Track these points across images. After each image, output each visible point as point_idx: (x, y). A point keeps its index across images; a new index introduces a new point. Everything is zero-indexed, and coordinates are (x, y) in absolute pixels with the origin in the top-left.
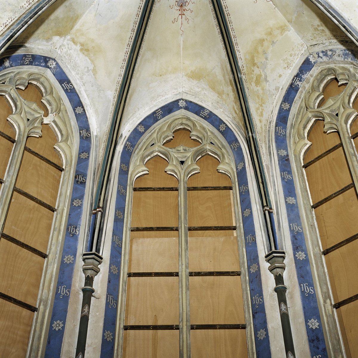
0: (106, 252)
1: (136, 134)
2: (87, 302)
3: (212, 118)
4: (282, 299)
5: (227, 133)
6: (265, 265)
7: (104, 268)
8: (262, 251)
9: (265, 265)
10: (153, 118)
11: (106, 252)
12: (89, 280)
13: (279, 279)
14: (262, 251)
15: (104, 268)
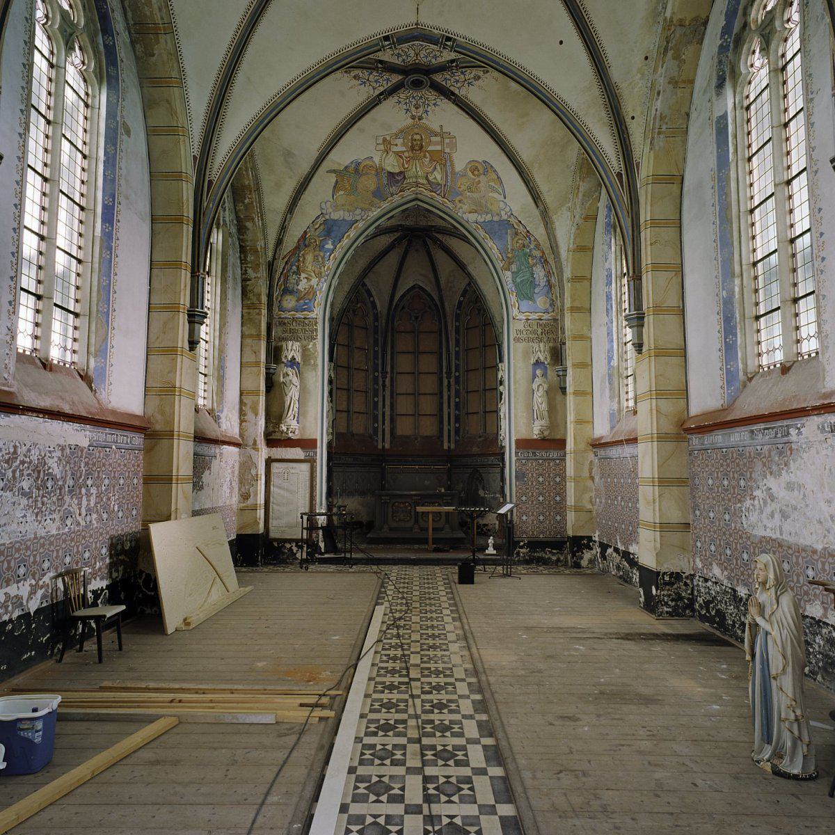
0: (389, 370)
1: (397, 306)
2: (384, 390)
3: (429, 295)
4: (449, 390)
5: (436, 305)
6: (445, 375)
7: (388, 375)
8: (444, 371)
9: (445, 375)
10: (403, 296)
11: (389, 370)
12: (384, 382)
13: (449, 382)
14: (444, 371)
15: (388, 375)
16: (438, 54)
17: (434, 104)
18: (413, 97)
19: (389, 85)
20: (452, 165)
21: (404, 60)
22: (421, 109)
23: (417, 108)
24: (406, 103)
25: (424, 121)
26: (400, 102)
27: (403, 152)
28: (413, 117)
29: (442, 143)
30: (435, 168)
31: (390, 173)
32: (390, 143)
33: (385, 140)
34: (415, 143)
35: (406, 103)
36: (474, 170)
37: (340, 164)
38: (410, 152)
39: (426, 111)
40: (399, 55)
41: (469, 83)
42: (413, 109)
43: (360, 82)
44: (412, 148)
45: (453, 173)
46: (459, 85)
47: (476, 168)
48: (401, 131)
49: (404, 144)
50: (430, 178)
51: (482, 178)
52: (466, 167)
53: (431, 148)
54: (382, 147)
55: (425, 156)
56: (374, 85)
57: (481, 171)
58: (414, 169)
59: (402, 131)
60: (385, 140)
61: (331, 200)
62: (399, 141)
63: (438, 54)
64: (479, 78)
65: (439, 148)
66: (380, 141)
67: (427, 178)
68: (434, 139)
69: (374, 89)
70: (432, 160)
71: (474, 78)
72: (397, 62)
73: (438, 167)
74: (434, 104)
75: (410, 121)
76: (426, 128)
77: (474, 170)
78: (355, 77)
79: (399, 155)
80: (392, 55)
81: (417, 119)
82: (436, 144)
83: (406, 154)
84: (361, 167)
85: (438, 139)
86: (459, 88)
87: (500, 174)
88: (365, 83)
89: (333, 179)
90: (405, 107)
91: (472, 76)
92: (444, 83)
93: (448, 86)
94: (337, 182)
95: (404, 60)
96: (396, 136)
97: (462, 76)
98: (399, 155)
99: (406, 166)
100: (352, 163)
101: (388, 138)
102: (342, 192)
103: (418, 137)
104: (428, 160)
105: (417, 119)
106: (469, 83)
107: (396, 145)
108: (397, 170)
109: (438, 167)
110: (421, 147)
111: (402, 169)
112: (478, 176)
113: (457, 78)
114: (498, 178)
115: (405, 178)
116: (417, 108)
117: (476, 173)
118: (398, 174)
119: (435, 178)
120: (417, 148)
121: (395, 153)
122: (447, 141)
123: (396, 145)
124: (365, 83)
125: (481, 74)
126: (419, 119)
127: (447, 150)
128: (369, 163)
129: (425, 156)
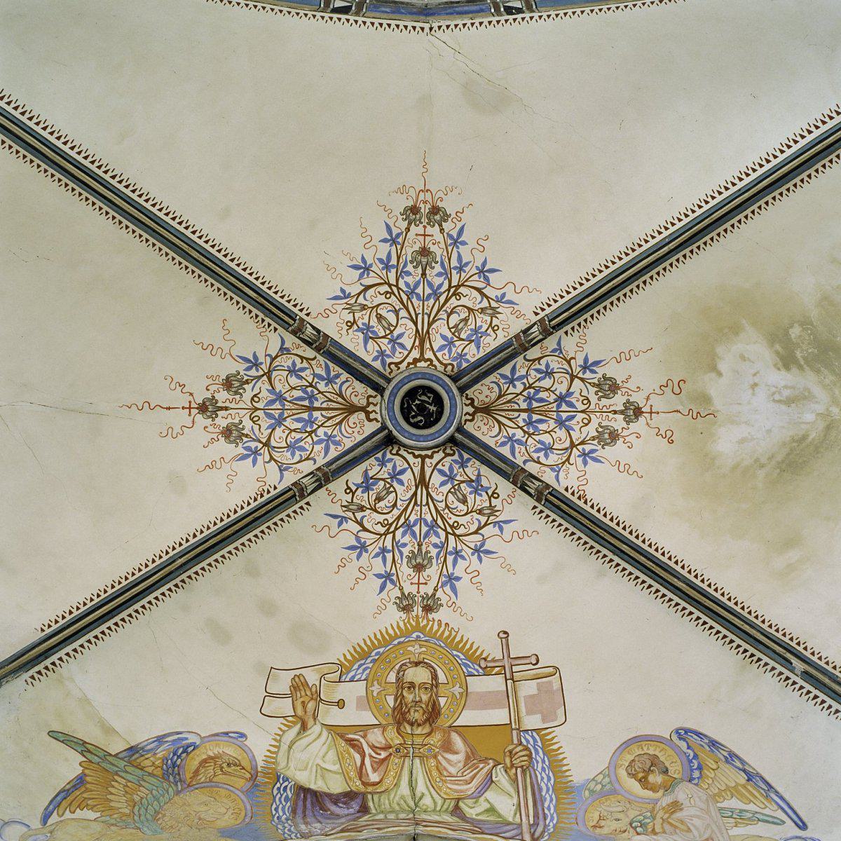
16: (482, 321)
17: (477, 550)
18: (409, 527)
19: (333, 453)
20: (556, 765)
21: (382, 354)
22: (433, 572)
23: (419, 568)
24: (384, 550)
25: (442, 615)
26: (362, 548)
27: (365, 728)
28: (405, 604)
29: (509, 698)
30: (489, 781)
31: (303, 791)
32: (317, 697)
33: (298, 685)
34: (409, 697)
35: (384, 550)
36: (648, 768)
37: (109, 731)
38: (392, 734)
39: (451, 579)
40: (368, 334)
41: (584, 455)
42: (405, 570)
43: (240, 450)
44: (400, 716)
45: (564, 788)
46: (553, 459)
47: (654, 761)
48: (362, 654)
49: (369, 701)
50: (473, 811)
51: (683, 793)
52: (613, 765)
53: (468, 717)
54: (286, 706)
55: (448, 747)
56: (286, 457)
57: (676, 769)
58: (404, 789)
59: (364, 655)
60: (298, 685)
61: (36, 824)
62: (353, 691)
63: (482, 321)
64: (614, 436)
65: (499, 716)
66: (283, 684)
67: (457, 811)
68: (479, 685)
69: (282, 469)
70: (472, 758)
71: (599, 437)
72: (361, 353)
73: (500, 776)
74: (477, 550)
75: (393, 617)
76: (451, 644)
77: (648, 768)
78: (227, 433)
79: (347, 737)
80: (351, 325)
81: (417, 610)
82: (487, 701)
83: (376, 737)
84: (193, 763)
85: (495, 683)
86: (556, 469)
87: (757, 763)
88: (256, 452)
89: (69, 766)
90: (378, 563)
91: (591, 430)
92: (505, 451)
93: (519, 461)
94: (80, 781)
95: (382, 354)
96: (343, 672)
97: (562, 433)
98: (347, 737)
99: (374, 777)
100: (160, 739)
101: (312, 678)
102: (91, 815)
103: (419, 675)
104: (460, 757)
105: (417, 610)
106: (584, 455)
107: (341, 704)
108: (336, 786)
109: (500, 776)
110: (433, 713)
111: (357, 786)
112: (668, 787)
113: (546, 439)
114: (751, 776)
115: (364, 809)
116: (419, 568)
117: (657, 778)
118: (335, 799)
119: (492, 810)
120: (416, 715)
121: (339, 732)
122: (528, 689)
123: (341, 704)
124: (256, 452)
125: (618, 423)
126: (428, 609)
127: (532, 721)
128: (231, 751)
129: (448, 747)
